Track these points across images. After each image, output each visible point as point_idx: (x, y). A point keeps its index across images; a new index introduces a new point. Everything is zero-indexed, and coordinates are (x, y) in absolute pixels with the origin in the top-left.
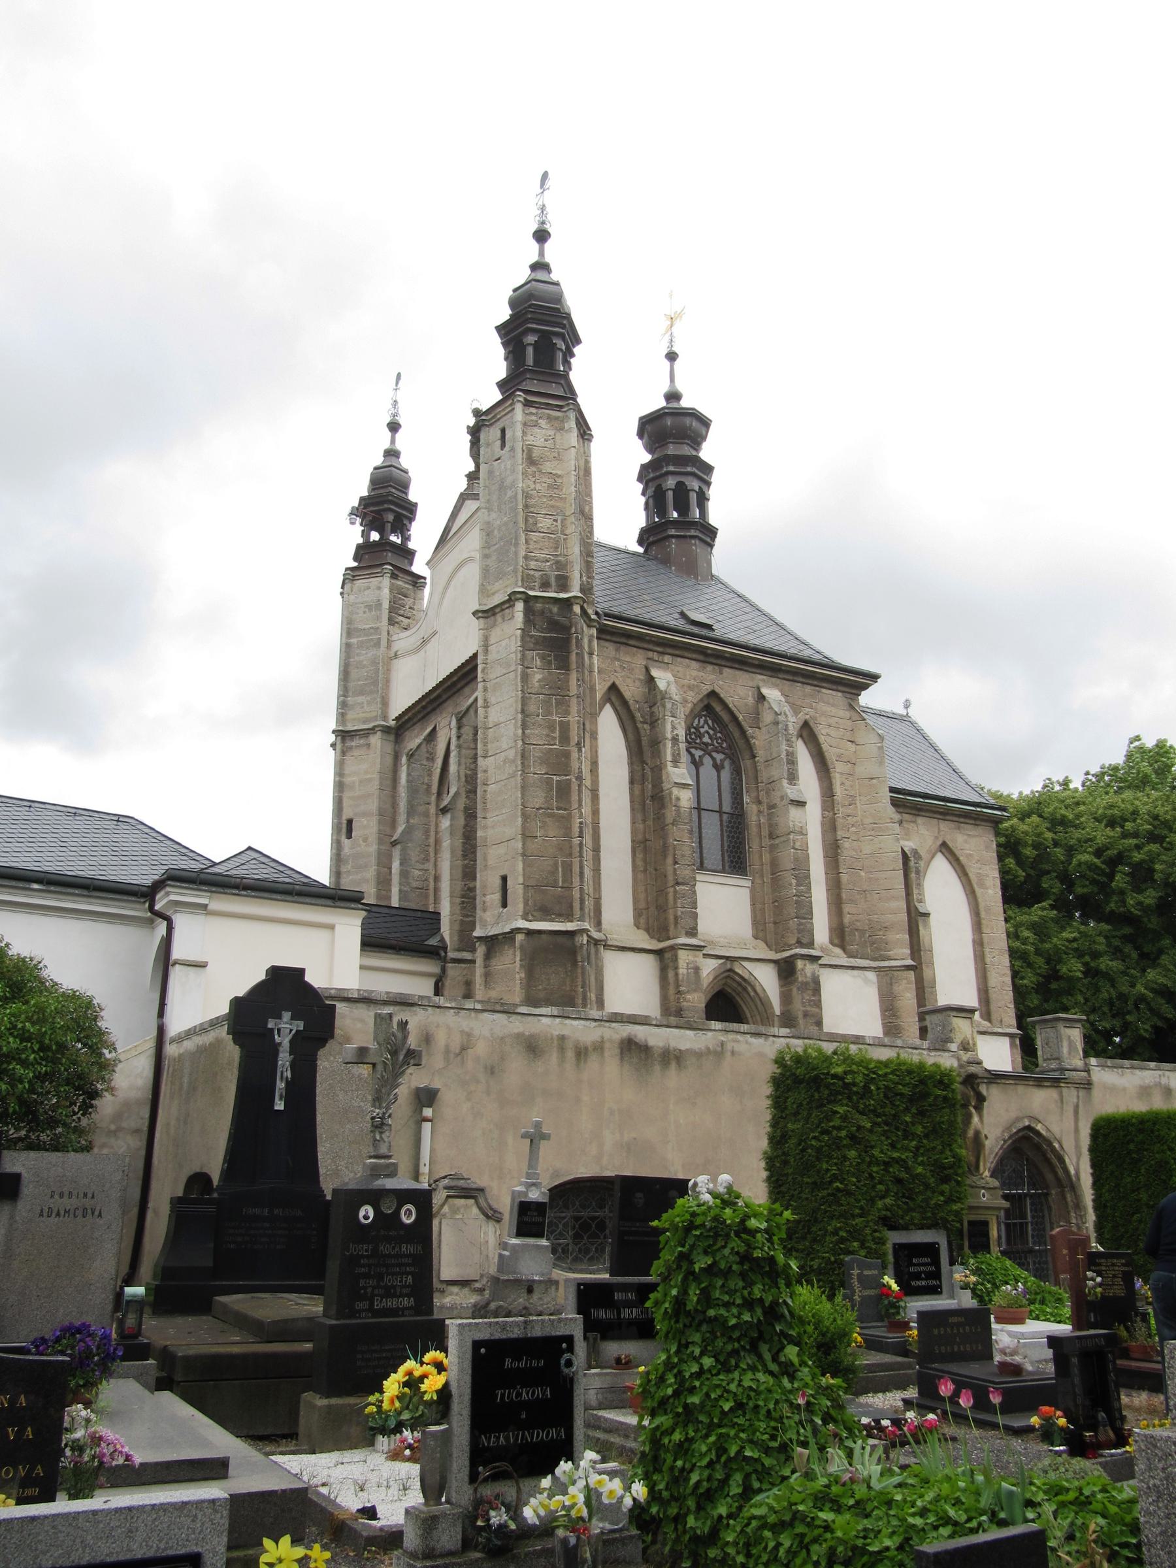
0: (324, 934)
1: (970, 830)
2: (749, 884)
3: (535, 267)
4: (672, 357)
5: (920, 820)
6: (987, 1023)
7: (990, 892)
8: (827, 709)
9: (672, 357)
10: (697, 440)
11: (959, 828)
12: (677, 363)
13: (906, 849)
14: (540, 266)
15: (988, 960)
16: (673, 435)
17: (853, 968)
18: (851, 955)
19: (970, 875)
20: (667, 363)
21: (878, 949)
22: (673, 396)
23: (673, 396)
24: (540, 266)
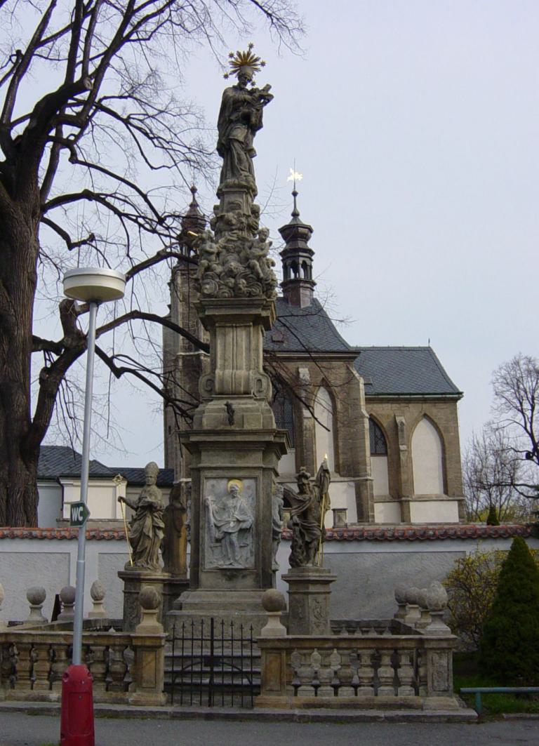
0: (111, 489)
1: (441, 406)
2: (294, 451)
3: (191, 206)
4: (295, 194)
5: (410, 405)
6: (446, 496)
7: (452, 434)
8: (337, 372)
9: (295, 194)
10: (306, 238)
11: (435, 406)
12: (297, 198)
13: (398, 421)
14: (194, 205)
15: (448, 466)
16: (295, 234)
17: (342, 482)
18: (341, 476)
19: (440, 427)
20: (293, 197)
21: (356, 473)
22: (295, 215)
23: (295, 215)
24: (194, 205)
